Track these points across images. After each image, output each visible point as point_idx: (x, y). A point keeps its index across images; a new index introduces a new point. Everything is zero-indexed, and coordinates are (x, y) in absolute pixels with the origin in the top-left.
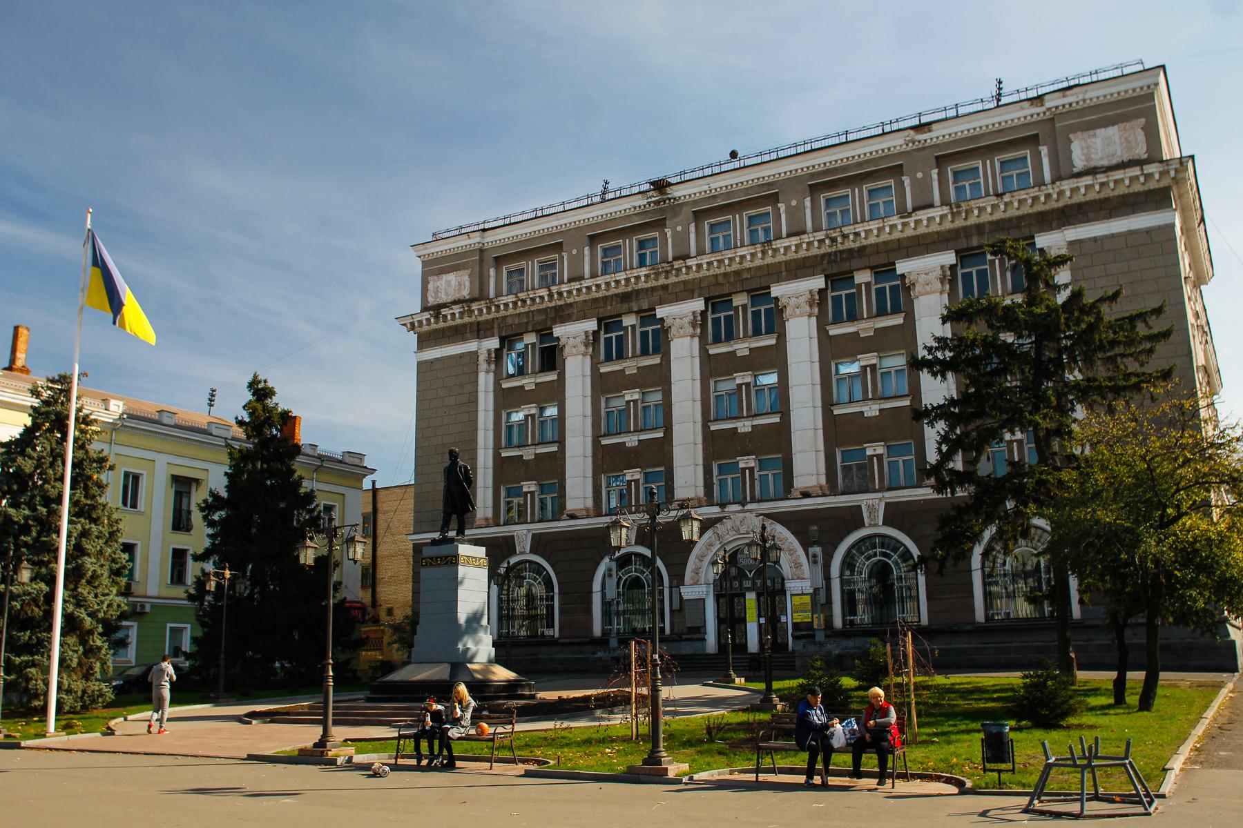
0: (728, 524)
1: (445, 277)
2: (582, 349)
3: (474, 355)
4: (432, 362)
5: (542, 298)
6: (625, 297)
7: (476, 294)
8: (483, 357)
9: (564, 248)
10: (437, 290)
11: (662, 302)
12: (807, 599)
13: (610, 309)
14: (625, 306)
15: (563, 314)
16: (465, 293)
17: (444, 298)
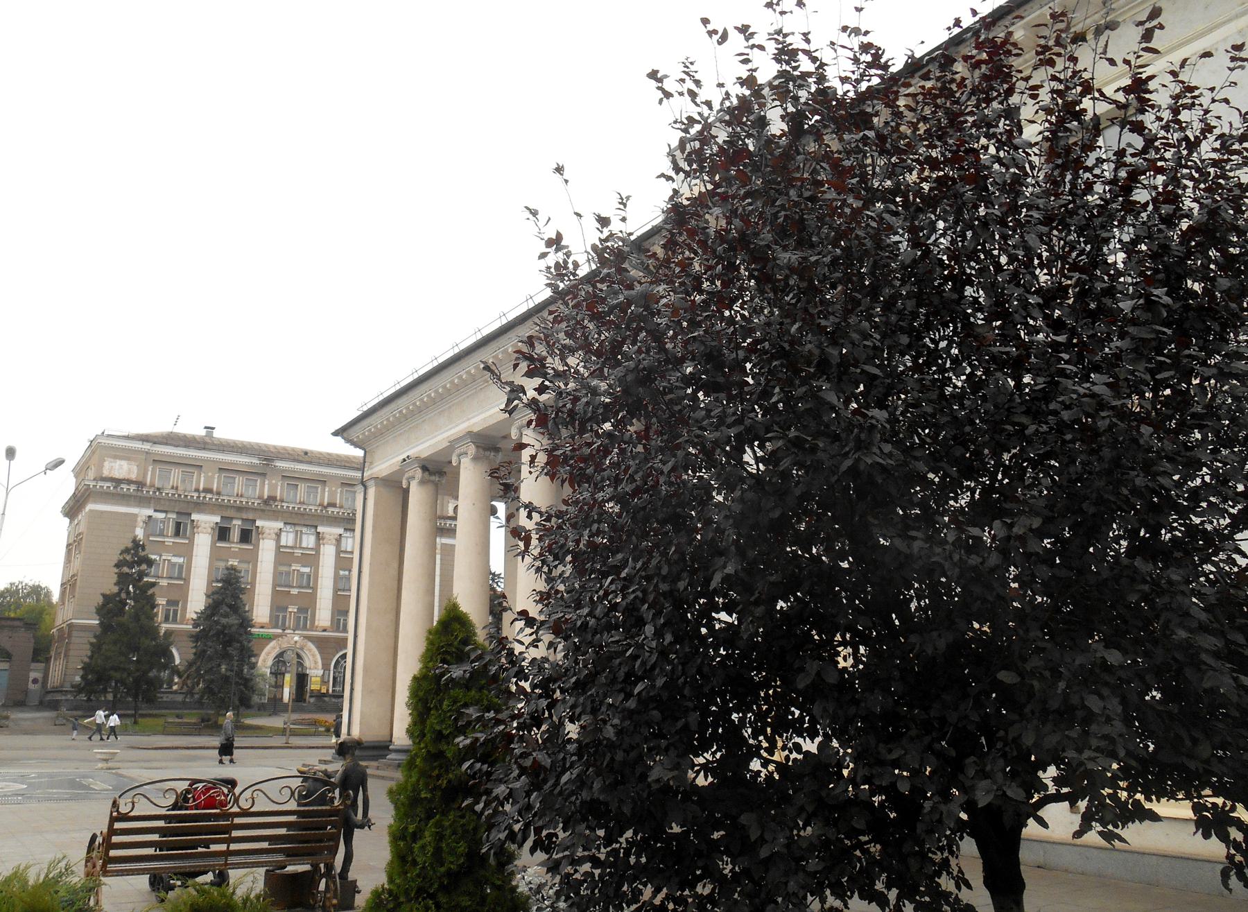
0: (286, 639)
1: (118, 462)
2: (210, 530)
3: (136, 516)
4: (102, 512)
5: (192, 497)
6: (240, 509)
7: (140, 479)
8: (139, 519)
9: (203, 469)
10: (111, 468)
11: (261, 518)
12: (319, 679)
13: (229, 513)
14: (238, 515)
15: (200, 506)
16: (133, 476)
17: (117, 474)
